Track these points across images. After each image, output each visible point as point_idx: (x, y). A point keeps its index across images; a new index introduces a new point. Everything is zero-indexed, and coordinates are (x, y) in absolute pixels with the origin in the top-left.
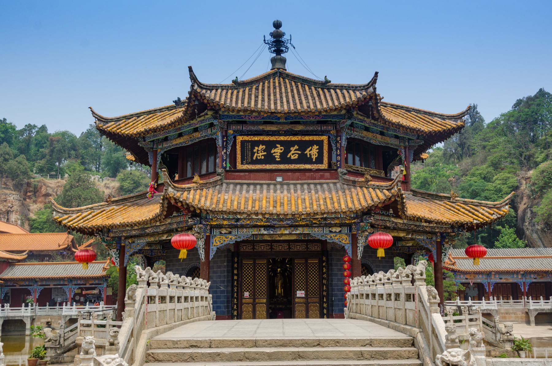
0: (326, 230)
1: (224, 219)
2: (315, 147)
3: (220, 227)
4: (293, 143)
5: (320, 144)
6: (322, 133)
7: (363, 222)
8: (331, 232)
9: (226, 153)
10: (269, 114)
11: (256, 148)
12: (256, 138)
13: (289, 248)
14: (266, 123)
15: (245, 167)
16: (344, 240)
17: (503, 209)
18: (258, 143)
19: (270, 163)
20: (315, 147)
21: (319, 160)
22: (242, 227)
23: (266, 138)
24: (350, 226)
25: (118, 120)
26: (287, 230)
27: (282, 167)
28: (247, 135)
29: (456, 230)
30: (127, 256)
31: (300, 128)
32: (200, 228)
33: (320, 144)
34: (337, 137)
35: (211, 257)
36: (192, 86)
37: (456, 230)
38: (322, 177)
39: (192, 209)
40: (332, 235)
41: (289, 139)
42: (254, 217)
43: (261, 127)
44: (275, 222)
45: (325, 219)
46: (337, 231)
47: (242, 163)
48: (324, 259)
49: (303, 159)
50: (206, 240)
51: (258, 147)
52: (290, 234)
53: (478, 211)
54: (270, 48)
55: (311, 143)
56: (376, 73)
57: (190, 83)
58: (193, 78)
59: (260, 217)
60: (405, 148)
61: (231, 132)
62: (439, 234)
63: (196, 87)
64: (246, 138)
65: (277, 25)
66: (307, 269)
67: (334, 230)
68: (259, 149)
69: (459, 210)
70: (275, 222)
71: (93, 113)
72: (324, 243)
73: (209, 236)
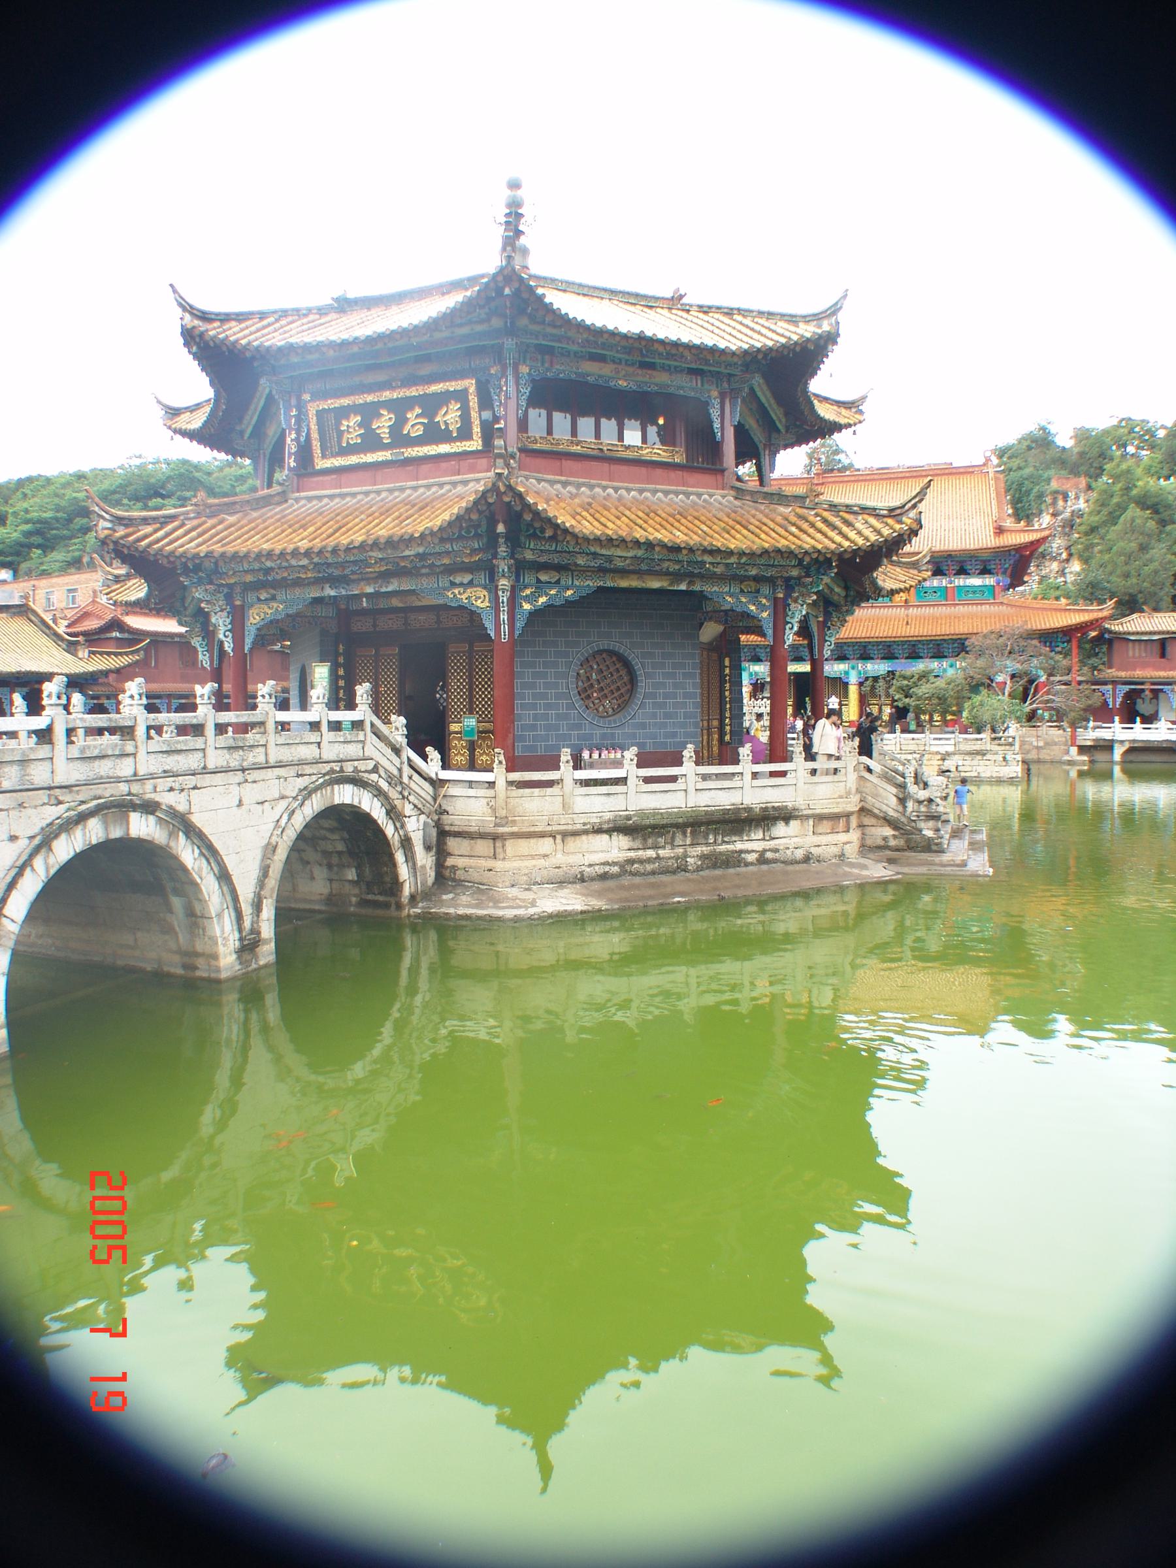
0: (444, 582)
1: (246, 572)
4: (409, 403)
5: (461, 396)
6: (462, 375)
11: (345, 423)
12: (345, 402)
13: (438, 622)
16: (480, 600)
17: (904, 519)
18: (343, 413)
21: (465, 433)
26: (369, 584)
31: (426, 370)
38: (472, 470)
40: (456, 591)
41: (401, 395)
43: (357, 380)
44: (330, 571)
46: (466, 581)
49: (434, 434)
51: (348, 419)
55: (444, 398)
59: (305, 562)
60: (722, 396)
62: (779, 582)
65: (514, 185)
66: (470, 664)
68: (351, 424)
69: (813, 525)
70: (330, 571)
73: (242, 607)
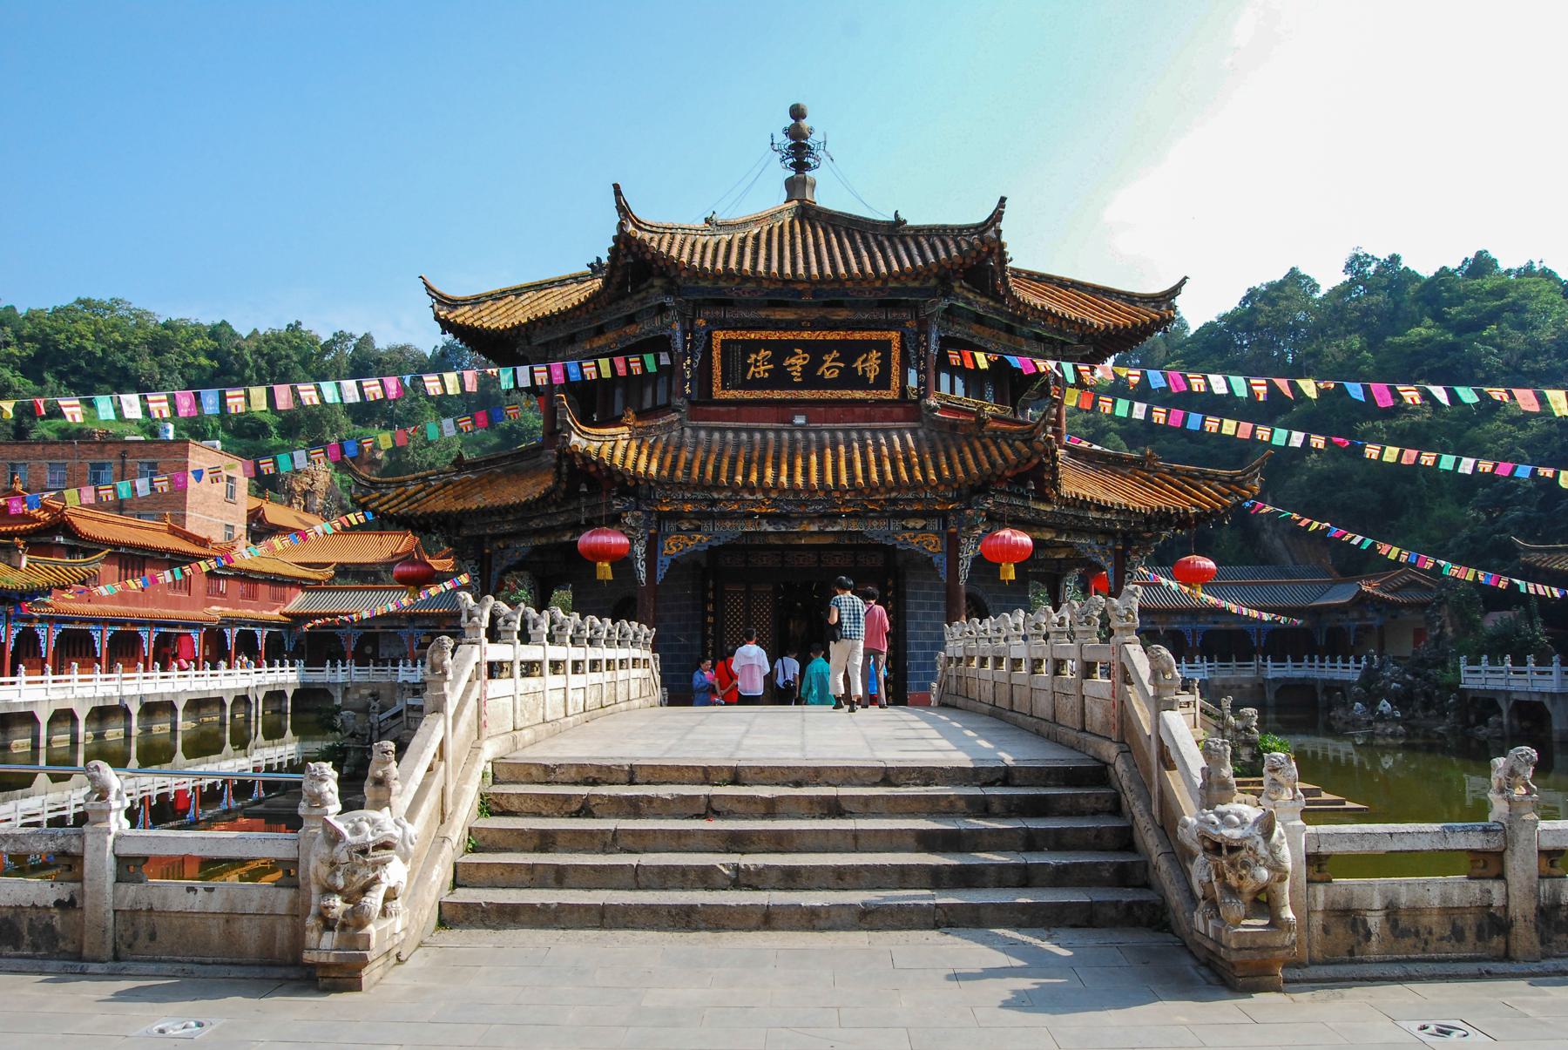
0: (895, 525)
1: (686, 501)
2: (875, 354)
3: (677, 516)
4: (827, 346)
5: (884, 347)
7: (970, 508)
8: (905, 528)
9: (690, 366)
10: (780, 285)
11: (753, 356)
14: (773, 304)
15: (731, 394)
16: (931, 544)
18: (756, 346)
19: (782, 388)
20: (875, 354)
22: (724, 516)
23: (774, 336)
24: (944, 516)
25: (477, 301)
27: (806, 394)
28: (735, 329)
29: (1154, 526)
30: (495, 574)
31: (842, 315)
32: (637, 519)
33: (884, 347)
34: (918, 334)
35: (659, 579)
36: (621, 225)
37: (1154, 526)
39: (618, 479)
42: (747, 496)
43: (763, 314)
45: (894, 502)
47: (724, 387)
48: (890, 583)
49: (850, 379)
50: (648, 543)
52: (821, 533)
53: (1198, 489)
54: (782, 160)
55: (867, 346)
56: (1003, 200)
57: (616, 219)
58: (623, 210)
59: (760, 496)
61: (701, 322)
63: (630, 228)
64: (732, 335)
65: (797, 113)
67: (911, 524)
71: (428, 287)
72: (890, 551)
